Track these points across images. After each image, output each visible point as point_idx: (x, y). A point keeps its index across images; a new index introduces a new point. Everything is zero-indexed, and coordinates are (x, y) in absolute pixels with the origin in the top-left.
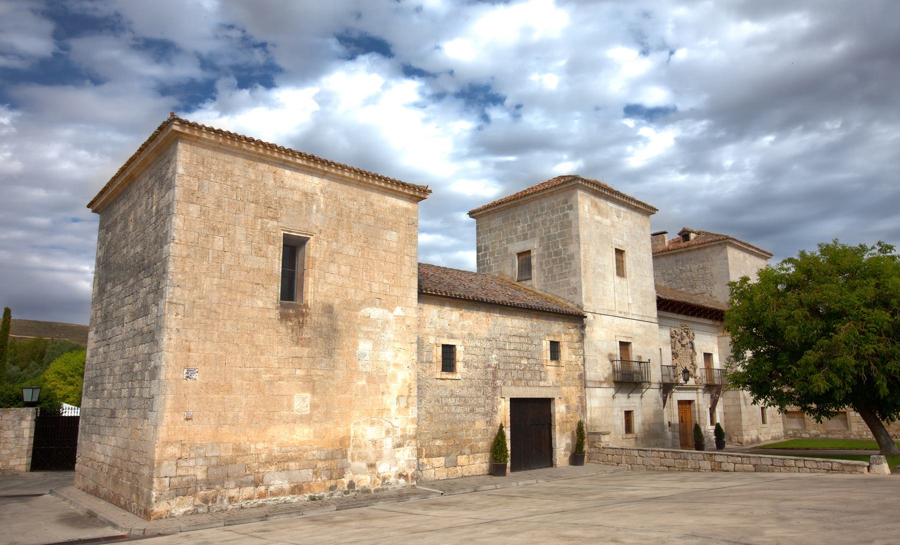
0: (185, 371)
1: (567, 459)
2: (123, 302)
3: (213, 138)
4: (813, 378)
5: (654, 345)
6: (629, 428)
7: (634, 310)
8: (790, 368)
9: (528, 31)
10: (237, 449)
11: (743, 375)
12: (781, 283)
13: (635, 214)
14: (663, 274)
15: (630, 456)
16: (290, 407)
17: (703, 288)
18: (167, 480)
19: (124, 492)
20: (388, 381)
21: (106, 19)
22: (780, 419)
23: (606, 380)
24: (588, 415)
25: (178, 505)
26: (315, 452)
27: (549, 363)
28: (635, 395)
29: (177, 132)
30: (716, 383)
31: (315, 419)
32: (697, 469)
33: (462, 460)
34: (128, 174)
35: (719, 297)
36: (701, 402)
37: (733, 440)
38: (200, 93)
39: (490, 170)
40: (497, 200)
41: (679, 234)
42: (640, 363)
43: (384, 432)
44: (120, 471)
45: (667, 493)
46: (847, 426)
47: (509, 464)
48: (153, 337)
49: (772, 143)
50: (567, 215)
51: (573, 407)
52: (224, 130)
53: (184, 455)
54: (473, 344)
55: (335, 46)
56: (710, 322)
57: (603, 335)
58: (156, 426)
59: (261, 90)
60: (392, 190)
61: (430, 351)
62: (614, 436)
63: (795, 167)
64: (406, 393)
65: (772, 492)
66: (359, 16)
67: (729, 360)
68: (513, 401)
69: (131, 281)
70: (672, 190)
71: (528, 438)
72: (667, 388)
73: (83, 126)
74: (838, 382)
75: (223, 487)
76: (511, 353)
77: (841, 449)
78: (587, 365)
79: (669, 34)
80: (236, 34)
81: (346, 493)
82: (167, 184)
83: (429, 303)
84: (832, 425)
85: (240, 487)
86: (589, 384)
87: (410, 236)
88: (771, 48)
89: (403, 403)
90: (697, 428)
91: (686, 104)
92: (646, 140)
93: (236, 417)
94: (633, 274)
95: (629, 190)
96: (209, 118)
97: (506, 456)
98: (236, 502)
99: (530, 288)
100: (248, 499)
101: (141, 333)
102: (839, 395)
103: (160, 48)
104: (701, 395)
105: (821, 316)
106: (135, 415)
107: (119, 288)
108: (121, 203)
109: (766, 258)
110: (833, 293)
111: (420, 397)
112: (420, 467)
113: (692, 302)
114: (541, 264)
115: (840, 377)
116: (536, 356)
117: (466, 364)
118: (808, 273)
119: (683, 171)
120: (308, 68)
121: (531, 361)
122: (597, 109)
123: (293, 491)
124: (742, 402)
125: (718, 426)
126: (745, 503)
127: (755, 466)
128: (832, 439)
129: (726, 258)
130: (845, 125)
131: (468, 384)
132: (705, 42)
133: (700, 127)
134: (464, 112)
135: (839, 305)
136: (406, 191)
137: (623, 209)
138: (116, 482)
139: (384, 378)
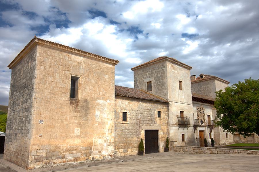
0: (39, 121)
1: (163, 150)
2: (19, 98)
3: (48, 44)
4: (243, 123)
5: (191, 112)
6: (183, 140)
7: (185, 101)
8: (236, 120)
9: (150, 9)
10: (56, 146)
11: (220, 122)
12: (232, 92)
13: (185, 69)
14: (194, 89)
15: (184, 149)
16: (73, 133)
17: (207, 94)
18: (33, 157)
19: (20, 161)
20: (105, 124)
21: (14, 5)
22: (232, 137)
23: (176, 124)
24: (170, 135)
25: (37, 165)
26: (81, 147)
27: (158, 118)
28: (185, 129)
29: (37, 42)
30: (212, 125)
31: (81, 137)
32: (205, 153)
33: (129, 150)
34: (21, 56)
35: (213, 97)
36: (206, 131)
37: (217, 144)
38: (44, 29)
39: (138, 55)
40: (140, 65)
41: (200, 76)
42: (187, 118)
43: (104, 141)
44: (18, 154)
45: (196, 161)
46: (254, 139)
47: (144, 152)
48: (29, 110)
49: (230, 46)
50: (163, 70)
51: (165, 133)
52: (52, 42)
53: (39, 148)
54: (133, 112)
55: (88, 14)
56: (210, 105)
57: (175, 109)
58: (30, 139)
59: (64, 29)
60: (106, 61)
61: (119, 114)
62: (178, 142)
63: (237, 54)
64: (111, 128)
65: (230, 160)
66: (96, 4)
67: (216, 117)
68: (146, 131)
69: (22, 91)
70: (197, 61)
71: (151, 142)
72: (195, 127)
73: (6, 40)
74: (251, 124)
75: (52, 159)
76: (145, 115)
77: (252, 146)
78: (170, 119)
79: (196, 10)
80: (56, 10)
81: (92, 161)
82: (33, 59)
83: (118, 99)
84: (249, 139)
85: (57, 159)
86: (170, 125)
87: (112, 76)
88: (229, 15)
89: (110, 132)
90: (205, 140)
91: (201, 33)
92: (189, 45)
93: (56, 136)
94: (184, 89)
95: (183, 61)
96: (47, 38)
97: (144, 149)
98: (56, 164)
99: (151, 94)
100: (60, 163)
101: (25, 108)
102: (251, 129)
103: (31, 15)
104: (206, 129)
105: (245, 103)
106: (23, 135)
107: (18, 94)
108: (19, 66)
109: (228, 84)
110: (249, 95)
111: (116, 129)
112: (115, 152)
113: (204, 98)
114: (155, 86)
115: (252, 123)
116: (153, 116)
117: (130, 118)
118: (241, 88)
119: (201, 55)
120: (79, 21)
121: (152, 118)
122: (173, 35)
123: (74, 161)
124: (220, 131)
125: (212, 139)
126: (221, 164)
127: (224, 152)
128: (249, 143)
129: (215, 84)
130: (253, 40)
131: (131, 125)
132: (208, 13)
133: (206, 41)
134: (130, 36)
135: (251, 99)
136: (111, 62)
137: (181, 68)
138: (17, 157)
139: (104, 123)
